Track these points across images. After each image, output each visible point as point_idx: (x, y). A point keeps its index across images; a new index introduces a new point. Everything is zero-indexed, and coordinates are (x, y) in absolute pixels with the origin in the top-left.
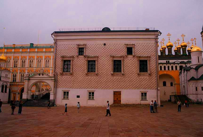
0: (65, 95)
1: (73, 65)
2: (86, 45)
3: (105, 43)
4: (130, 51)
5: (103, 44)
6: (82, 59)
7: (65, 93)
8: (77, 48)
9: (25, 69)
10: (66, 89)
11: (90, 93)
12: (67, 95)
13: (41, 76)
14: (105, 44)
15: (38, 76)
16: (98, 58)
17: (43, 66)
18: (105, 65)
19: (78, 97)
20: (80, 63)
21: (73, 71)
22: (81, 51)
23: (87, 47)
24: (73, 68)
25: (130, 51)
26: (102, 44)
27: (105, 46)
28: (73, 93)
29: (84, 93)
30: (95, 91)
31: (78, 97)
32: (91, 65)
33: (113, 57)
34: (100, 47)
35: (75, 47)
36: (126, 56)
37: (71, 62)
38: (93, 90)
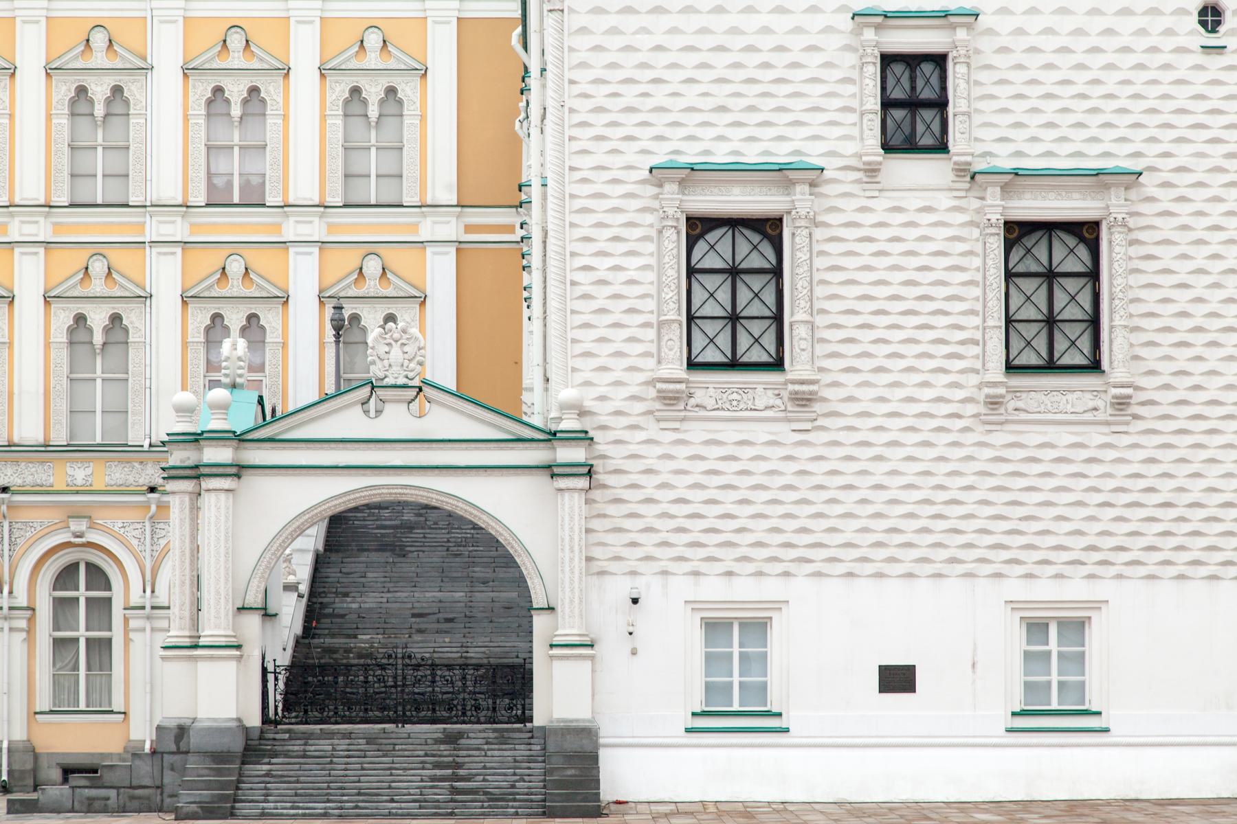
1: (817, 277)
6: (928, 209)
7: (714, 628)
8: (851, 59)
13: (396, 420)
16: (1133, 194)
19: (897, 679)
20: (898, 266)
21: (827, 363)
23: (985, 44)
24: (820, 320)
26: (1181, 11)
28: (822, 640)
29: (968, 634)
31: (897, 679)
34: (1154, 50)
35: (837, 41)
38: (1075, 590)
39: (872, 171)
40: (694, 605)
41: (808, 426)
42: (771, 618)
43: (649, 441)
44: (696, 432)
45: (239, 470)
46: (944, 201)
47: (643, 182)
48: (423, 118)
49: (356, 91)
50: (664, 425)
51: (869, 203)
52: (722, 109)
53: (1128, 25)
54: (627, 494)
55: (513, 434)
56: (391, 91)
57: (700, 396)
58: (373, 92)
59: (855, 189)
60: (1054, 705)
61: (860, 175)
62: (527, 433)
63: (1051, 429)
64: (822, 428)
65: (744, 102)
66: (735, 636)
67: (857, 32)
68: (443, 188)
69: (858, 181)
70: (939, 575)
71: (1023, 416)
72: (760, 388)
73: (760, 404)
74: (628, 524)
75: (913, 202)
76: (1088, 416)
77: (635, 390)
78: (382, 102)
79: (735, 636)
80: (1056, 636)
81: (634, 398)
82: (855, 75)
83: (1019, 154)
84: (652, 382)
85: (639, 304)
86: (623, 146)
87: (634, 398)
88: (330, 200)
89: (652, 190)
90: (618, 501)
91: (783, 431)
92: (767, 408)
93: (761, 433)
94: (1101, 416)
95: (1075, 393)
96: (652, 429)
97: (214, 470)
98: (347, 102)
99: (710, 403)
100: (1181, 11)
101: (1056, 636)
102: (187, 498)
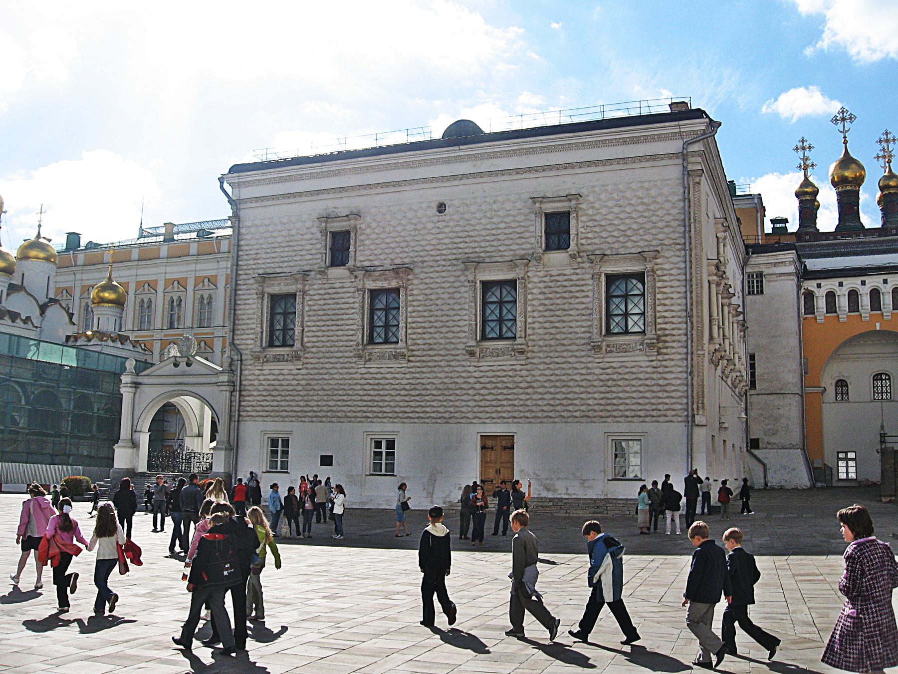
0: (274, 453)
2: (358, 215)
3: (442, 199)
4: (557, 229)
5: (435, 205)
9: (152, 336)
12: (283, 451)
14: (441, 208)
17: (189, 324)
18: (442, 309)
25: (557, 229)
27: (442, 217)
32: (382, 311)
33: (473, 263)
37: (299, 300)
40: (264, 432)
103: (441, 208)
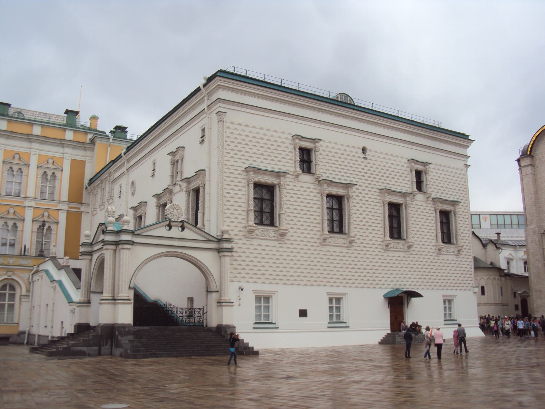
5: (361, 148)
6: (309, 188)
7: (258, 299)
10: (265, 288)
11: (331, 300)
13: (176, 232)
14: (364, 150)
15: (162, 231)
19: (303, 313)
22: (306, 159)
26: (359, 148)
30: (345, 294)
31: (303, 313)
36: (414, 196)
38: (340, 290)
39: (297, 176)
41: (282, 242)
42: (271, 296)
43: (244, 244)
44: (255, 242)
45: (132, 243)
46: (312, 186)
47: (243, 171)
48: (61, 181)
49: (45, 172)
50: (248, 239)
51: (296, 184)
52: (262, 154)
53: (348, 149)
54: (238, 258)
55: (206, 238)
56: (54, 173)
57: (256, 232)
58: (50, 173)
59: (293, 180)
60: (336, 319)
61: (293, 177)
62: (212, 239)
63: (336, 248)
64: (286, 243)
65: (267, 154)
66: (264, 300)
67: (293, 140)
68: (65, 197)
69: (293, 178)
70: (312, 285)
71: (330, 244)
72: (271, 231)
73: (272, 235)
74: (238, 267)
75: (306, 185)
76: (343, 245)
77: (241, 229)
78: (51, 176)
79: (264, 300)
80: (335, 302)
81: (240, 231)
82: (293, 151)
83: (328, 177)
84: (245, 227)
85: (242, 204)
86: (238, 160)
87: (240, 231)
88: (37, 197)
89: (245, 173)
90: (236, 260)
91: (276, 243)
92: (274, 237)
93: (271, 243)
94: (346, 245)
95: (339, 239)
96: (244, 241)
97: (126, 242)
98: (43, 175)
99: (259, 234)
100: (359, 148)
101: (335, 302)
102: (112, 251)
103: (364, 150)
